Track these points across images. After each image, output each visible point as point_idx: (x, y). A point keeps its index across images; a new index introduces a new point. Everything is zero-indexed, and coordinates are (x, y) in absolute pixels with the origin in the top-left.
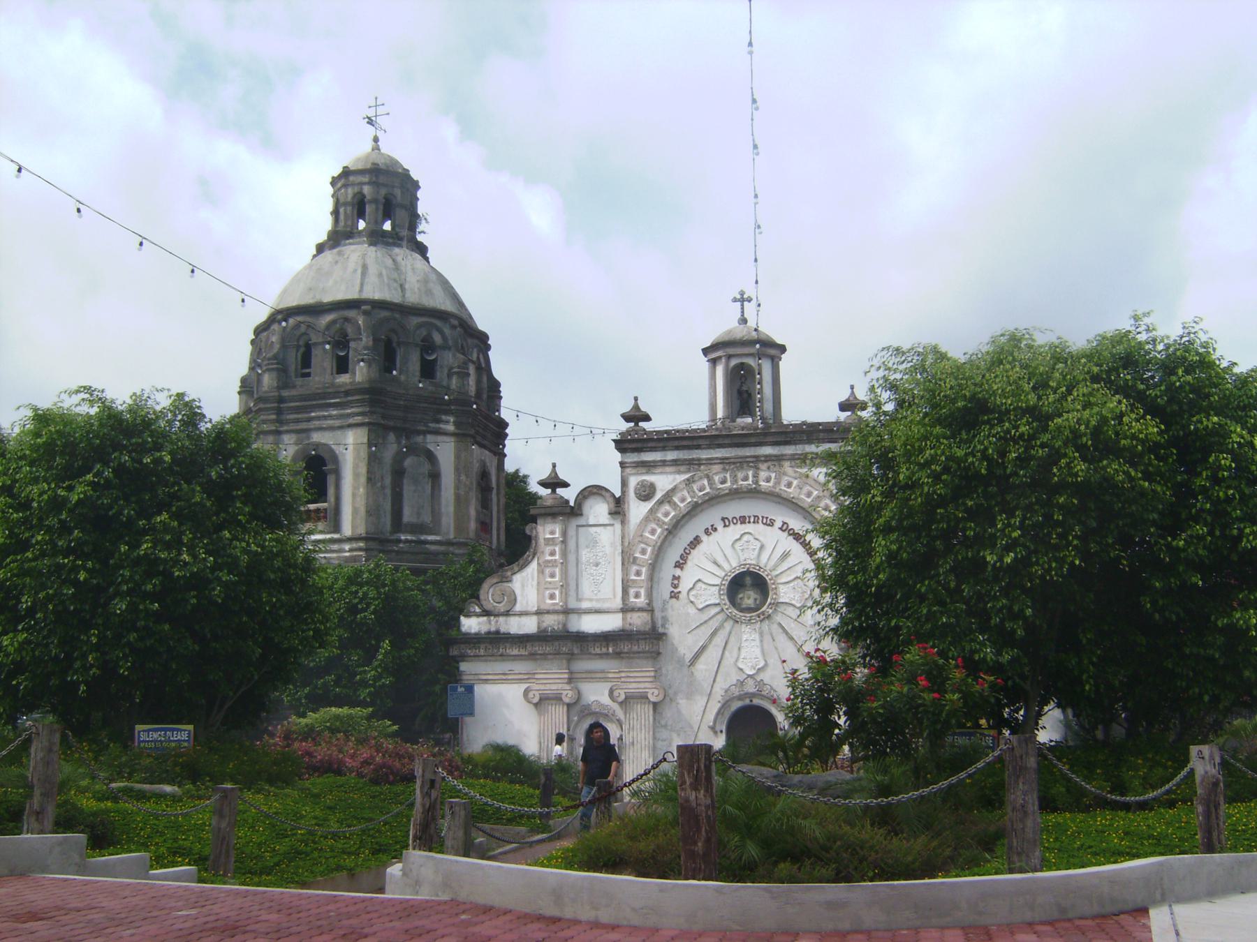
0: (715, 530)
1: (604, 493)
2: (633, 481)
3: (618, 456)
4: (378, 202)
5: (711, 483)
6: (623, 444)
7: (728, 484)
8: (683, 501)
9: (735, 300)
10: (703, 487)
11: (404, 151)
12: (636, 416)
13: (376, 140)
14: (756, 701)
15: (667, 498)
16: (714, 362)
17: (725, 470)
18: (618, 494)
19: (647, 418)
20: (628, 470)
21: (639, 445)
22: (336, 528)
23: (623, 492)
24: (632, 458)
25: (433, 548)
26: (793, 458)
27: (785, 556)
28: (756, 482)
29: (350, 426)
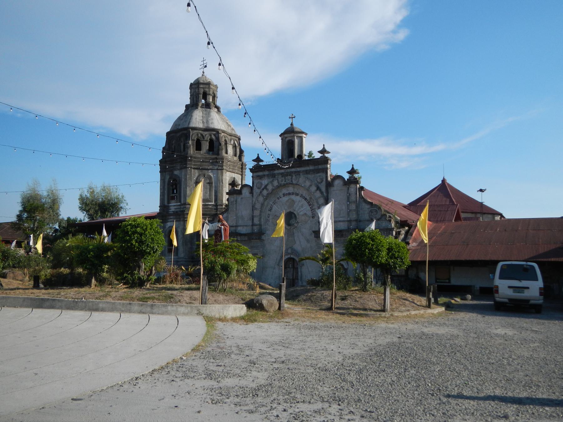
2: (256, 181)
3: (251, 174)
5: (278, 182)
7: (283, 182)
8: (270, 187)
10: (276, 183)
13: (203, 72)
14: (292, 256)
15: (266, 187)
16: (282, 139)
19: (262, 161)
22: (180, 202)
24: (255, 174)
25: (210, 206)
26: (303, 171)
27: (302, 206)
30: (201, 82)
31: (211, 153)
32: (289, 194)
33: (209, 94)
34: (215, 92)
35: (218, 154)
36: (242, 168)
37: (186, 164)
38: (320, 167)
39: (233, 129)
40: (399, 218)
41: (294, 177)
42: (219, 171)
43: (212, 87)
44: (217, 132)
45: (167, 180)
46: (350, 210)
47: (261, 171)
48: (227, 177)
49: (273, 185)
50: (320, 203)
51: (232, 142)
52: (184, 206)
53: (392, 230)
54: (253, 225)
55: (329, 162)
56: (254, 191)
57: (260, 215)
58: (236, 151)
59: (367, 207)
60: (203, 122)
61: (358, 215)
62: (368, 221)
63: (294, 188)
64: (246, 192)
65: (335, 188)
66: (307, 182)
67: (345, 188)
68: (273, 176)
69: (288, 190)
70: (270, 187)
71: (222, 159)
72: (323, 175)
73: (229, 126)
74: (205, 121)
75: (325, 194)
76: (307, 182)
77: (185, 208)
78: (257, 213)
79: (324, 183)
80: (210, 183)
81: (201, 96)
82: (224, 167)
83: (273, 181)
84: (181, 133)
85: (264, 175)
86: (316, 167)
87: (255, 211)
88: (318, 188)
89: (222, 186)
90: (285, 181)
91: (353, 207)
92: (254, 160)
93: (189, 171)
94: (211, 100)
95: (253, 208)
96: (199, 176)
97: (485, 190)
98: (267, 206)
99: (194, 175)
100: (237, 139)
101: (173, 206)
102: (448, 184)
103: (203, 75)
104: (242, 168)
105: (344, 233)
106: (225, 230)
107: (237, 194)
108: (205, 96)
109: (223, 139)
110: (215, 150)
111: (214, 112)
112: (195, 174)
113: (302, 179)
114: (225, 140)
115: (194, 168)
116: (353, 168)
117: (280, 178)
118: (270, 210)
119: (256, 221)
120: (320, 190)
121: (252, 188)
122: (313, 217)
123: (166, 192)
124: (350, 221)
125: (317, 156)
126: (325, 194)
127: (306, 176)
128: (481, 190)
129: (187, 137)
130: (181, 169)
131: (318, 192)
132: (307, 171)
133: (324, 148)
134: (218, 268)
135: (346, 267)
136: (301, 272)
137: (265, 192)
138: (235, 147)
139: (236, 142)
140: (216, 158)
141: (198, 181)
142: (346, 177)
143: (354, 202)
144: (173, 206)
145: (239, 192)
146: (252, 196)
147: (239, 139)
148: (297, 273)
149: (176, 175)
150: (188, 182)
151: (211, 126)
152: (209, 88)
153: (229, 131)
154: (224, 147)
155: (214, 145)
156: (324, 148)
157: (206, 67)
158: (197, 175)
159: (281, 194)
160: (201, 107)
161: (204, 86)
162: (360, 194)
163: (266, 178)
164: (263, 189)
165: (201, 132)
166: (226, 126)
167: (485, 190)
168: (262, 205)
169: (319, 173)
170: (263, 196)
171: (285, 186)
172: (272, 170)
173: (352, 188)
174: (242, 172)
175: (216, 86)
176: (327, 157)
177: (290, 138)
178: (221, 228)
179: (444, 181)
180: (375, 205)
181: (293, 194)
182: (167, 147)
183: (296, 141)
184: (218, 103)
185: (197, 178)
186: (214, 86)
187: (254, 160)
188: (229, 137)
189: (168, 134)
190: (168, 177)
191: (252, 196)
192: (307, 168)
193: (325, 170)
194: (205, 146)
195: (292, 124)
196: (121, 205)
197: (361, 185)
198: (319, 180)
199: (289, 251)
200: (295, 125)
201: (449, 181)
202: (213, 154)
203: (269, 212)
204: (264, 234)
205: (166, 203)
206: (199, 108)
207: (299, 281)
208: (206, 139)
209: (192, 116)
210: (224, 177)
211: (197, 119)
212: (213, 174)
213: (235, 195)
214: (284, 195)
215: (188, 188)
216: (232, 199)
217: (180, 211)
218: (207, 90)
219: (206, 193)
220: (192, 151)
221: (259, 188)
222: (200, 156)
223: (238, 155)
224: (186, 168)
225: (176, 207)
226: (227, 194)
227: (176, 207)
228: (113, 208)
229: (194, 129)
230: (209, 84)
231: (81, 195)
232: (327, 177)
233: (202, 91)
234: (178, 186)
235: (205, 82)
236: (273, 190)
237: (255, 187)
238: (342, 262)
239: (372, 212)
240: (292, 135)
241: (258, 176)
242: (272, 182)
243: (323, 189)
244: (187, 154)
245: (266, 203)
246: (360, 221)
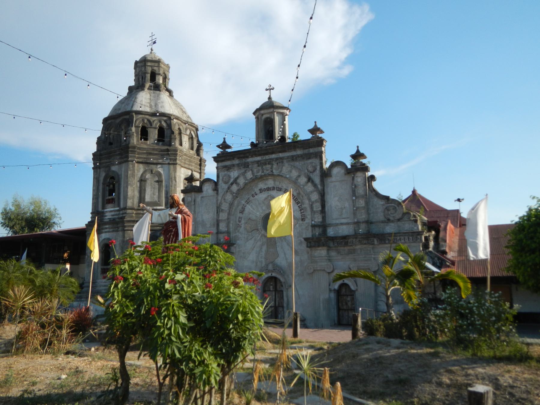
0: (256, 194)
3: (215, 164)
4: (149, 74)
5: (253, 174)
6: (216, 159)
7: (260, 173)
8: (241, 181)
9: (267, 90)
10: (249, 175)
11: (160, 53)
12: (224, 146)
13: (152, 50)
14: (274, 275)
15: (235, 181)
16: (257, 118)
17: (258, 166)
18: (216, 180)
19: (229, 147)
20: (219, 170)
21: (223, 159)
22: (119, 205)
23: (218, 180)
24: (221, 164)
26: (288, 157)
28: (272, 171)
29: (123, 163)
30: (149, 58)
31: (161, 143)
32: (268, 189)
33: (159, 74)
34: (166, 73)
35: (170, 145)
36: (200, 165)
37: (127, 157)
38: (311, 150)
39: (188, 117)
40: (426, 219)
41: (275, 166)
42: (172, 167)
43: (162, 66)
44: (168, 117)
45: (102, 179)
46: (357, 208)
47: (228, 160)
48: (182, 173)
49: (245, 178)
50: (313, 200)
51: (188, 132)
52: (124, 211)
53: (420, 233)
54: (218, 233)
55: (324, 143)
56: (219, 187)
57: (228, 219)
58: (192, 144)
59: (382, 202)
60: (151, 107)
61: (369, 214)
62: (383, 222)
63: (274, 181)
64: (208, 189)
65: (333, 179)
66: (294, 171)
67: (349, 178)
68: (246, 166)
69: (266, 184)
70: (241, 181)
71: (176, 150)
72: (316, 161)
73: (184, 112)
74: (153, 104)
75: (319, 186)
76: (294, 171)
77: (126, 213)
78: (223, 216)
79: (318, 171)
80: (159, 182)
81: (148, 76)
82: (178, 162)
83: (245, 172)
84: (121, 119)
85: (233, 165)
86: (306, 151)
87: (221, 214)
88: (310, 180)
89: (175, 185)
90: (263, 172)
91: (361, 203)
92: (218, 146)
93: (131, 166)
94: (161, 82)
95: (219, 210)
96: (145, 172)
97: (463, 200)
98: (238, 206)
99: (138, 171)
100: (194, 129)
101: (110, 212)
102: (420, 195)
103: (151, 53)
104: (200, 165)
105: (349, 240)
106: (184, 221)
107: (195, 192)
108: (153, 76)
109: (177, 127)
110: (166, 140)
111: (164, 95)
112: (139, 170)
113: (286, 169)
114: (179, 129)
115: (138, 162)
116: (358, 151)
117: (255, 168)
118: (242, 212)
119: (223, 227)
120: (313, 182)
121: (216, 184)
122: (303, 220)
123: (100, 194)
124: (357, 223)
125: (309, 136)
126: (319, 186)
127: (292, 163)
128: (459, 200)
129: (129, 123)
130: (120, 163)
131: (310, 184)
132: (293, 156)
133: (316, 125)
134: (176, 322)
135: (353, 288)
136: (287, 296)
137: (235, 188)
138: (191, 138)
139: (192, 132)
140: (168, 150)
141: (143, 178)
142: (349, 162)
143: (362, 197)
144: (110, 212)
145: (199, 190)
146: (217, 194)
147: (197, 129)
148: (282, 298)
149: (114, 171)
150: (130, 180)
151: (162, 110)
152: (159, 66)
153: (184, 118)
154: (177, 137)
155: (165, 133)
156: (316, 125)
157: (155, 43)
158: (142, 171)
159: (258, 192)
160: (148, 89)
161: (153, 64)
162: (370, 186)
163: (236, 168)
164: (232, 184)
165: (147, 117)
166: (181, 113)
167: (463, 200)
168: (231, 205)
169: (310, 158)
170: (232, 193)
171: (262, 178)
172: (244, 157)
173: (359, 178)
174: (200, 169)
175: (168, 66)
176: (321, 138)
177: (268, 116)
178: (175, 218)
179: (414, 192)
180: (394, 200)
181: (274, 188)
182: (103, 137)
183: (277, 119)
184: (170, 87)
185: (142, 175)
186: (164, 65)
187: (218, 146)
188: (184, 126)
189: (105, 121)
190: (103, 175)
191: (217, 194)
192: (293, 153)
193: (319, 155)
194: (154, 134)
195: (270, 98)
196: (55, 220)
197: (369, 174)
198: (310, 169)
199: (270, 267)
200: (274, 99)
201: (419, 192)
202: (163, 145)
203: (241, 215)
204: (233, 244)
205: (100, 209)
206: (146, 90)
207: (285, 309)
208: (154, 126)
209: (136, 98)
210: (178, 174)
211: (144, 101)
212: (164, 170)
213: (193, 194)
214: (261, 191)
215: (129, 187)
216: (190, 199)
217: (119, 218)
218: (155, 68)
219: (154, 194)
220: (135, 140)
221: (226, 183)
222: (145, 146)
223: (195, 148)
224: (127, 161)
225: (113, 213)
226: (183, 191)
227: (113, 213)
228: (43, 223)
229: (138, 113)
230: (158, 62)
231: (5, 209)
232: (321, 164)
233: (149, 70)
234: (116, 186)
235: (154, 59)
236: (246, 184)
237: (220, 182)
238: (346, 281)
239: (388, 210)
240: (271, 110)
241: (225, 167)
242: (244, 174)
243: (317, 180)
244: (129, 143)
245: (236, 202)
246: (371, 223)
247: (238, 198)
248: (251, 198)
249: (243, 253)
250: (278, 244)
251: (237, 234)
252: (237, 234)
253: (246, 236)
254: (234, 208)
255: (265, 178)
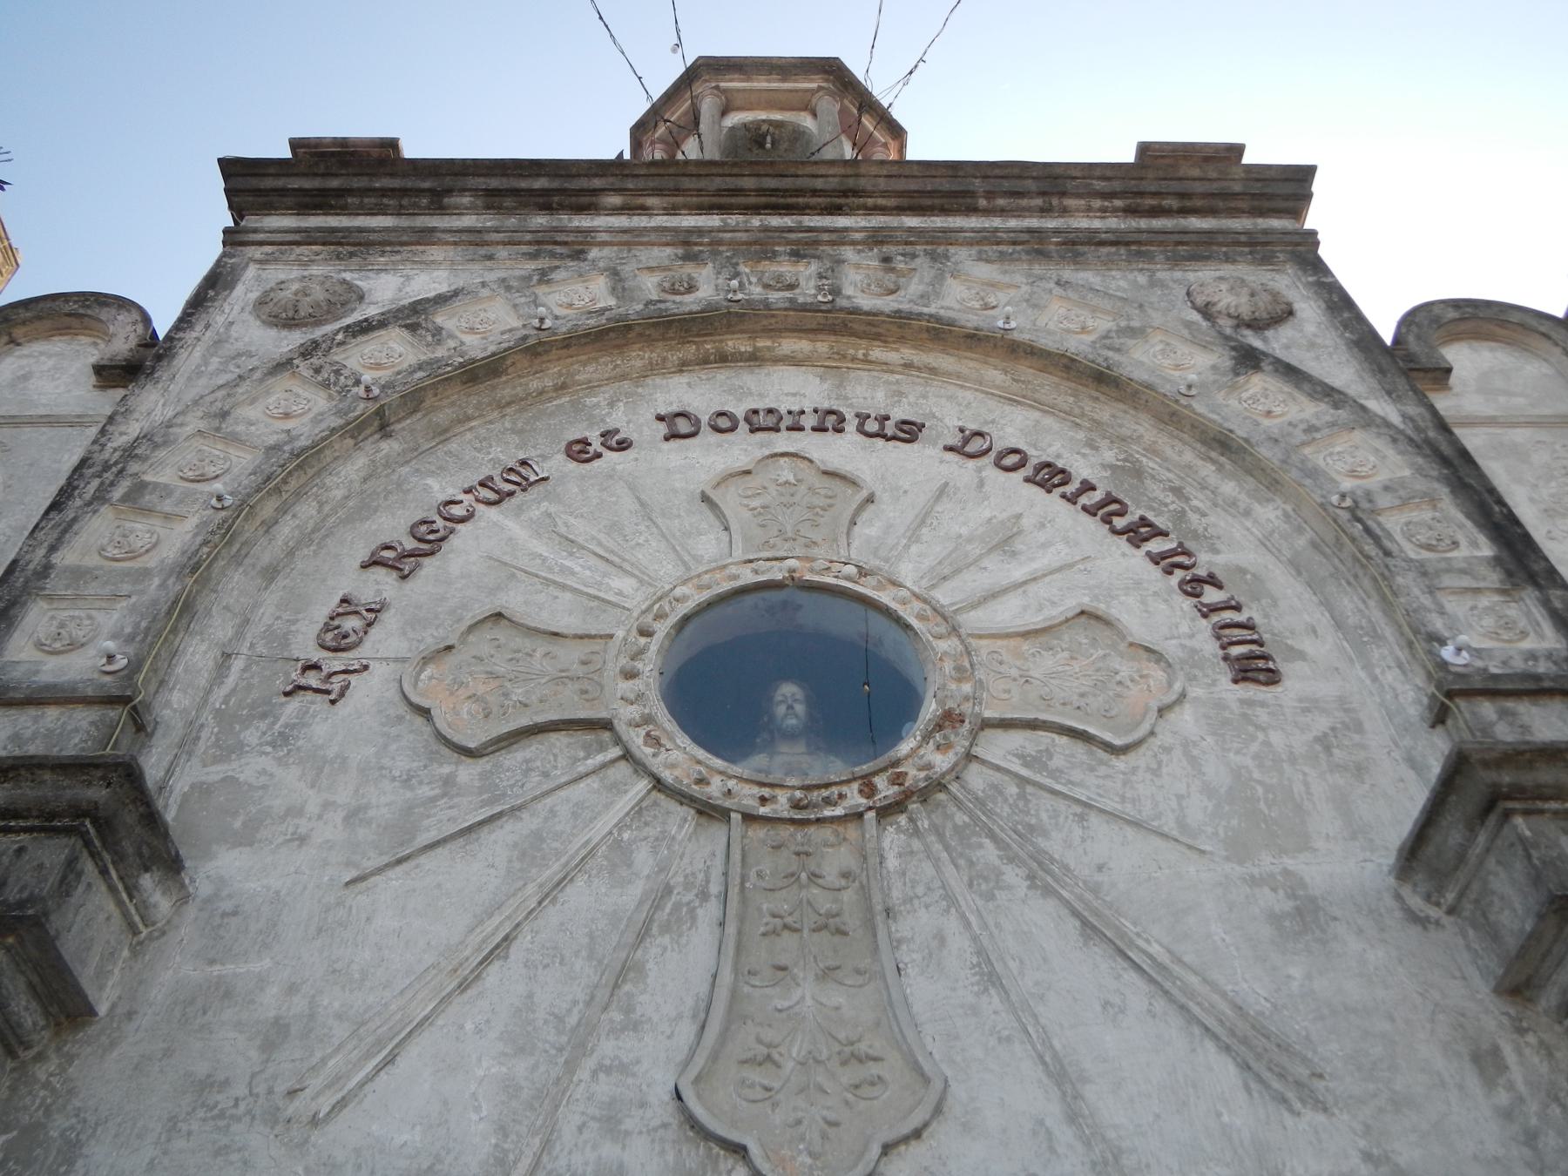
0: (624, 445)
1: (105, 314)
98: (364, 508)
214: (679, 427)
245: (351, 469)
247: (388, 447)
248: (556, 464)
249: (275, 1035)
250: (917, 924)
251: (249, 769)
252: (249, 769)
253: (385, 800)
254: (307, 510)
255: (737, 344)
